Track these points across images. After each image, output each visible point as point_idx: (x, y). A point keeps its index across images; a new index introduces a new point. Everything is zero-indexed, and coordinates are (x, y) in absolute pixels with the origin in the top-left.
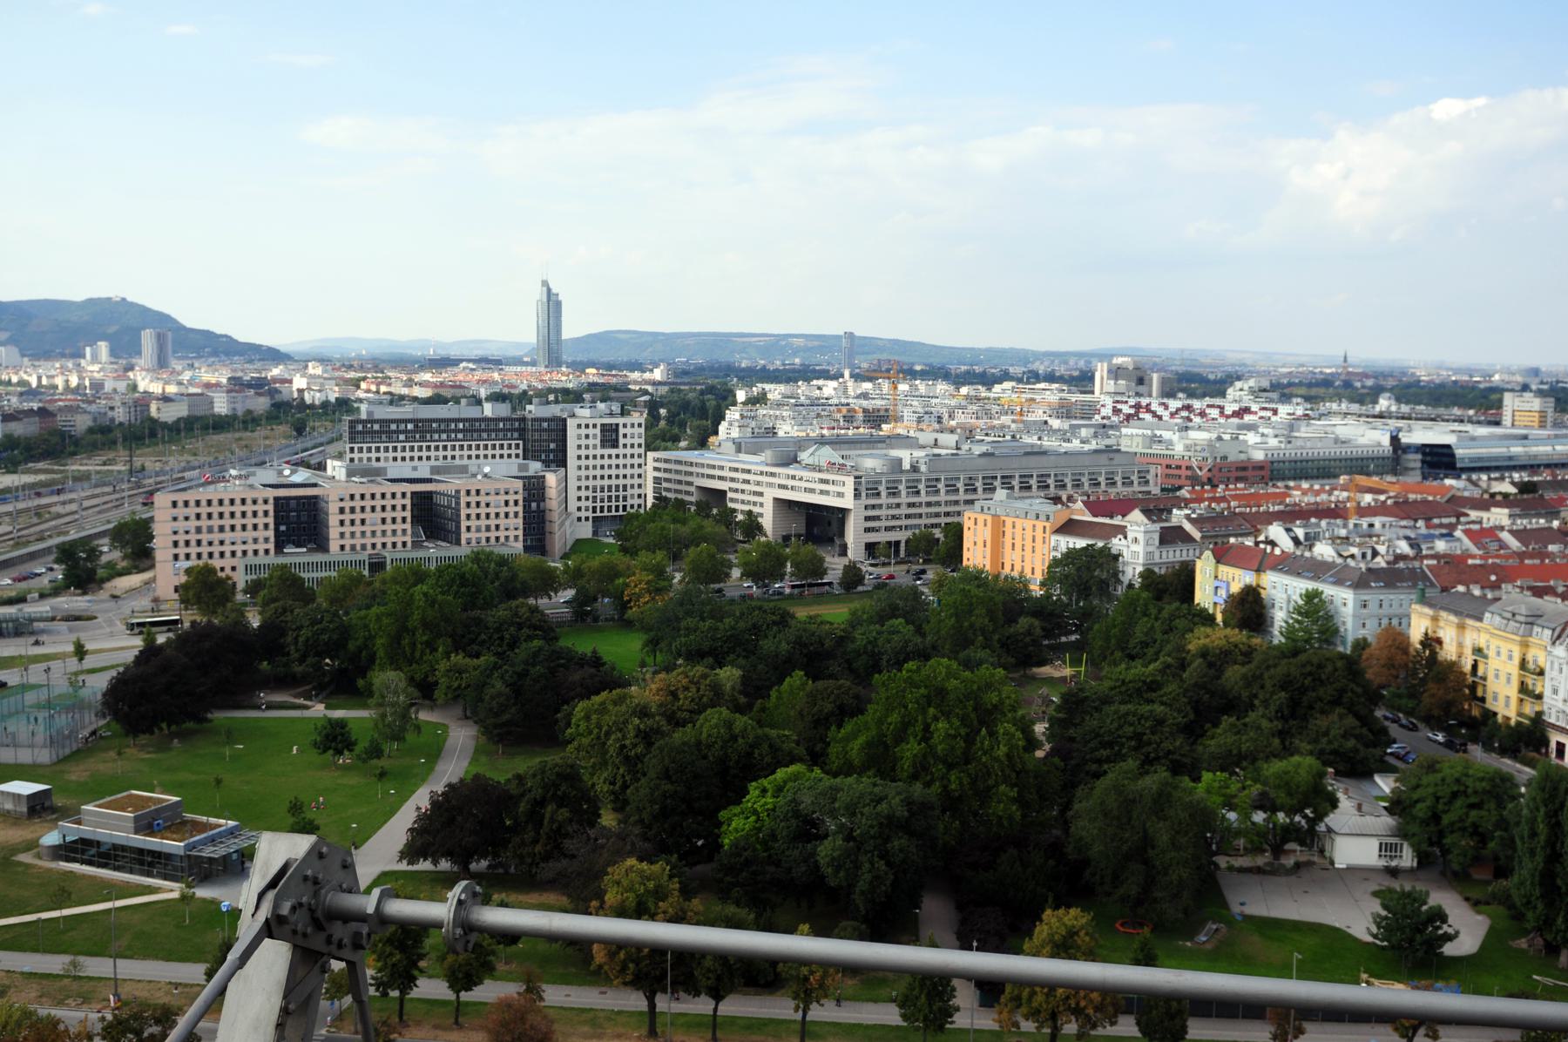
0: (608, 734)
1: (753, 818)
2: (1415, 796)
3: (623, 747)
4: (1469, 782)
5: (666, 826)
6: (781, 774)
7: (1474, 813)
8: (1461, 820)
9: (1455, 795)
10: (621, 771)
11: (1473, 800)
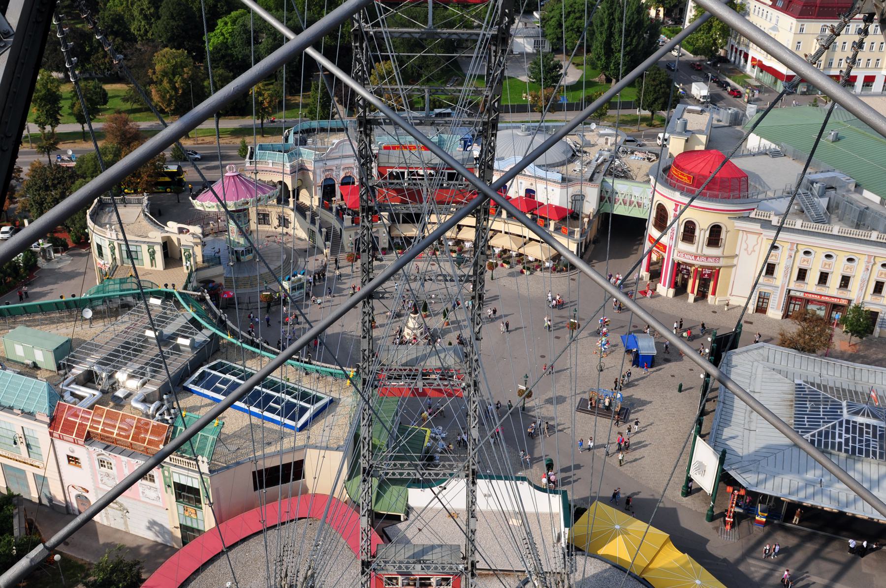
0: (132, 4)
1: (221, 38)
2: (551, 15)
3: (142, 9)
4: (576, 7)
5: (176, 44)
6: (234, 14)
7: (578, 21)
8: (572, 25)
9: (569, 13)
10: (143, 23)
11: (578, 15)
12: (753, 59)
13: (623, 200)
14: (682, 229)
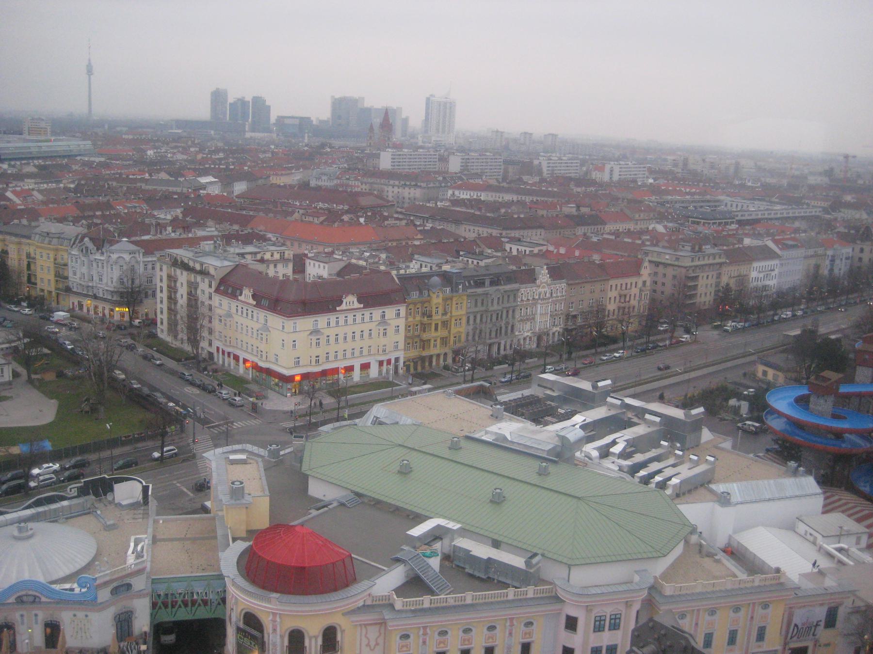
12: (245, 361)
13: (182, 601)
14: (286, 643)
